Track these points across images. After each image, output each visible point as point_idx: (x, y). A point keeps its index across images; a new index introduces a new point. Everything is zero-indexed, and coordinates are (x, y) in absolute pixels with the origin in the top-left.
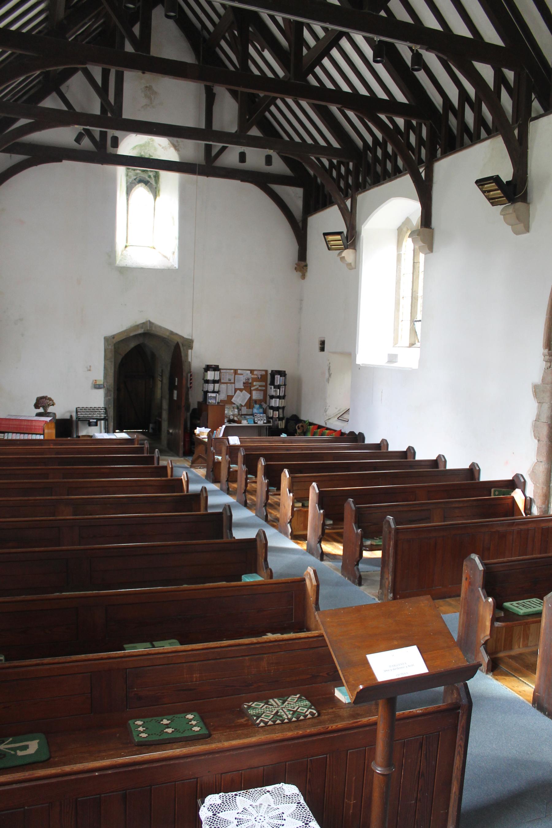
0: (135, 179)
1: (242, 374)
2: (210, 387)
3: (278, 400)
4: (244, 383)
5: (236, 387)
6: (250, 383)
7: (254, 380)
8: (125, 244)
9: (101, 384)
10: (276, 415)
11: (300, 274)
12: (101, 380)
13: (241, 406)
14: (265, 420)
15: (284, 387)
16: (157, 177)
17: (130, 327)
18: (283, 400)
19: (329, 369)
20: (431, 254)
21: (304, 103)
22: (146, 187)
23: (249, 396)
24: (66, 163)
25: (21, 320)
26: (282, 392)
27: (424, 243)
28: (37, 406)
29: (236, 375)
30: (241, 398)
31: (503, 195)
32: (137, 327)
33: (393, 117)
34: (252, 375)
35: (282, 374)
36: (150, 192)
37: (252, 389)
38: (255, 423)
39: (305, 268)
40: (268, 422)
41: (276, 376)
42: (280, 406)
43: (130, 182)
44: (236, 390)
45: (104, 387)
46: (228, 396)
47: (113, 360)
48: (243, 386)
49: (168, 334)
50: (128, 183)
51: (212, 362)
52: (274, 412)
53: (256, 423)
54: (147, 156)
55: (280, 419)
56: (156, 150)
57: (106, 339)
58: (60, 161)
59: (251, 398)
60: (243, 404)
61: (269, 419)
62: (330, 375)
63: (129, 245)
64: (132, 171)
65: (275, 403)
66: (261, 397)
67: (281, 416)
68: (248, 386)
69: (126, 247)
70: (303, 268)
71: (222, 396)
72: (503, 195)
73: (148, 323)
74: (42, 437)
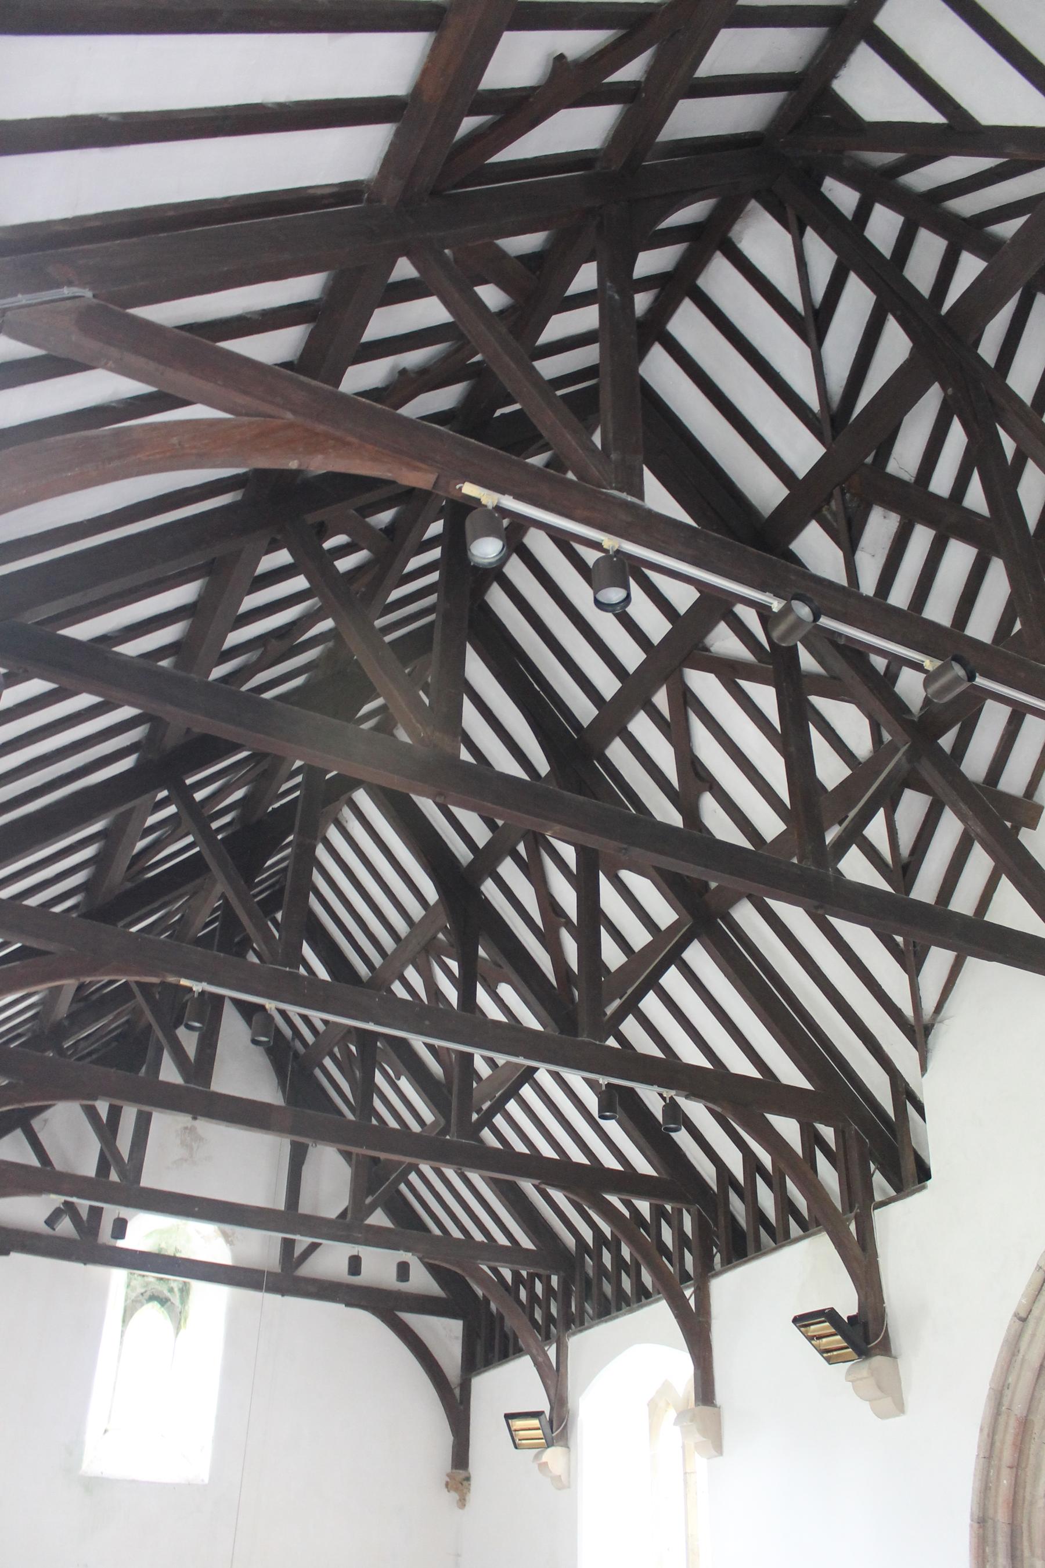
0: (142, 1294)
11: (455, 1496)
16: (185, 1291)
20: (721, 1458)
21: (475, 1177)
31: (846, 1344)
33: (633, 1201)
39: (465, 1483)
43: (133, 1298)
50: (129, 1301)
54: (170, 1252)
70: (462, 1484)
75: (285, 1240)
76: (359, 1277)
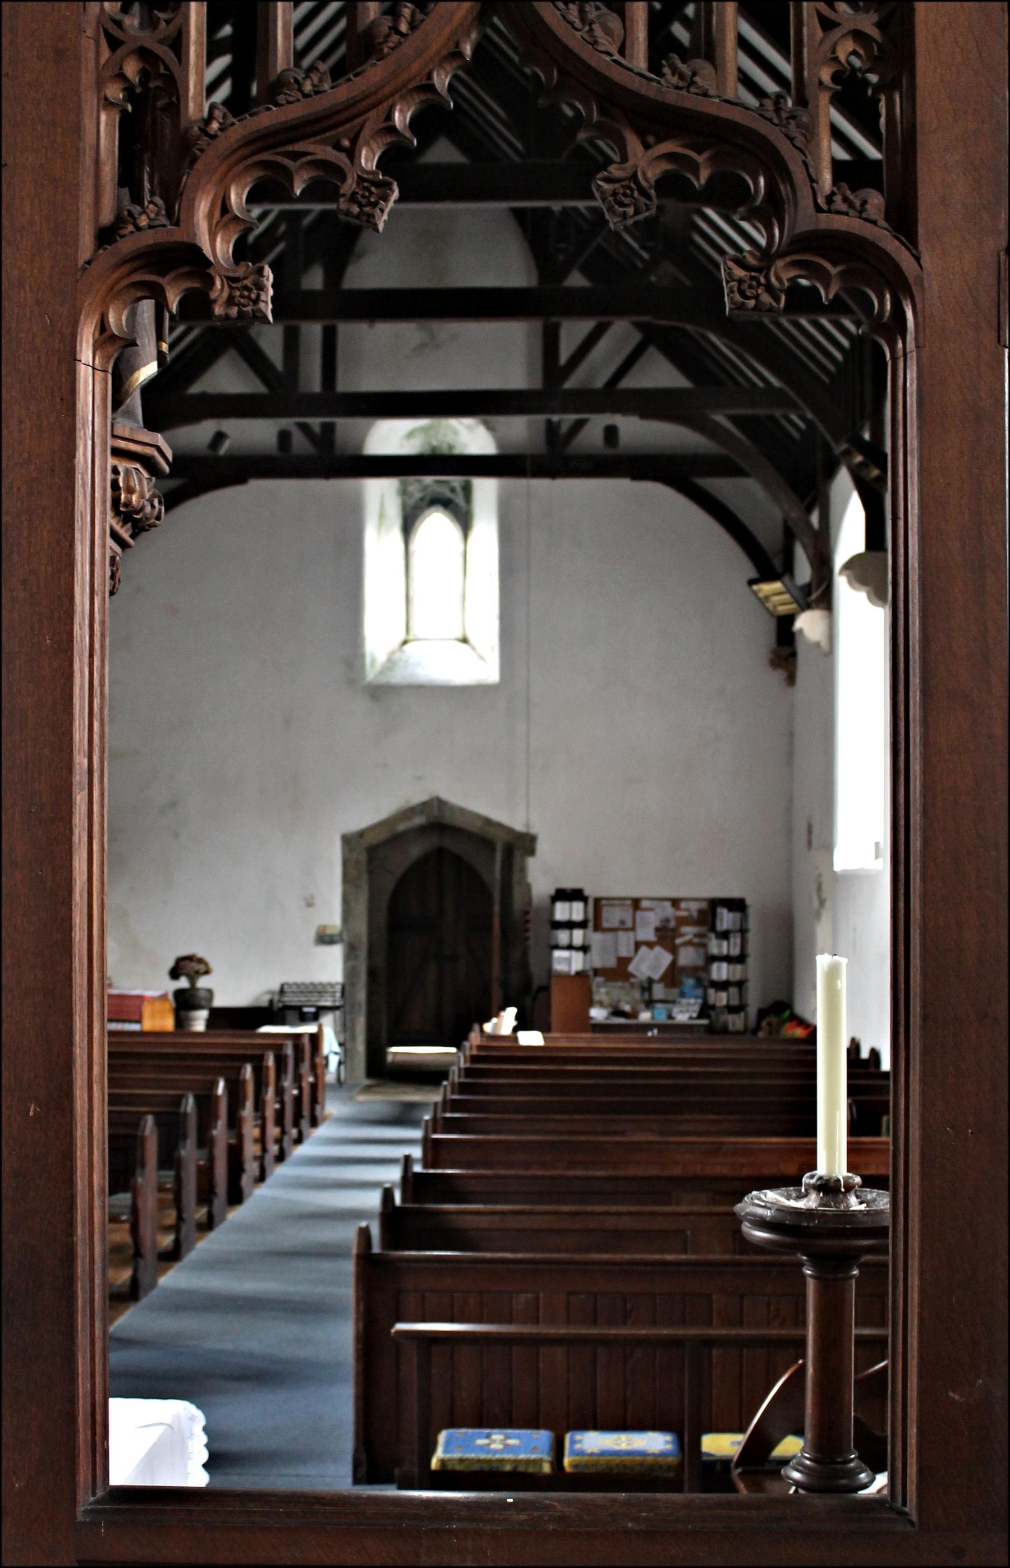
1: (650, 909)
2: (563, 936)
6: (673, 930)
7: (682, 921)
8: (402, 637)
10: (721, 1000)
11: (780, 675)
12: (334, 927)
13: (651, 981)
16: (467, 490)
19: (819, 889)
24: (256, 486)
25: (173, 804)
26: (735, 945)
28: (175, 973)
29: (639, 914)
35: (737, 905)
37: (679, 941)
40: (701, 1015)
44: (638, 945)
45: (341, 941)
49: (479, 823)
51: (569, 884)
55: (731, 1009)
56: (456, 433)
57: (348, 841)
59: (673, 964)
60: (656, 976)
61: (706, 1010)
62: (822, 903)
65: (719, 970)
66: (700, 962)
67: (735, 1002)
69: (405, 642)
71: (597, 959)
73: (435, 803)
74: (135, 1027)
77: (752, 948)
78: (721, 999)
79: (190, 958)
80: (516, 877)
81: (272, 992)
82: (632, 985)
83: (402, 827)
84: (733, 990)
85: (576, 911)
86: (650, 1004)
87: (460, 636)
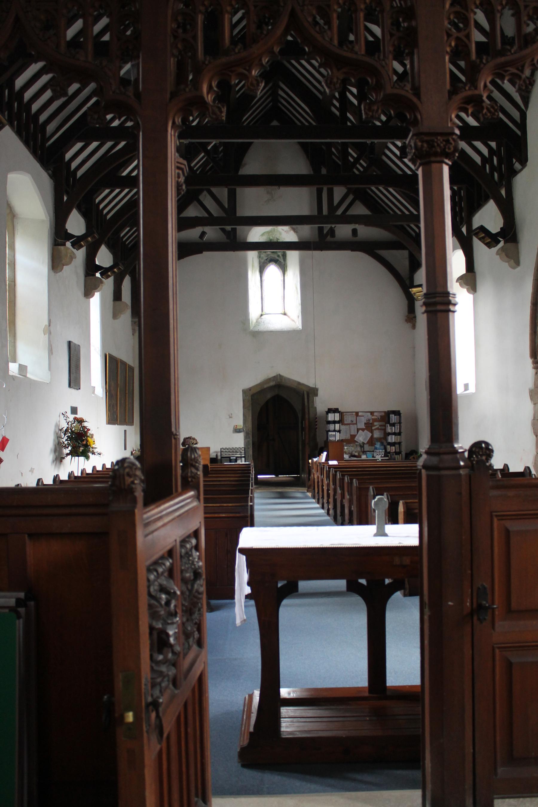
0: (266, 260)
2: (331, 427)
3: (394, 436)
4: (365, 424)
5: (358, 428)
6: (371, 424)
7: (375, 420)
8: (260, 313)
9: (241, 429)
10: (392, 450)
11: (410, 325)
12: (241, 425)
13: (364, 443)
14: (383, 454)
15: (399, 424)
16: (284, 256)
17: (263, 380)
18: (399, 436)
22: (276, 264)
23: (371, 434)
27: (468, 286)
29: (358, 417)
30: (362, 437)
31: (490, 240)
32: (269, 380)
34: (372, 416)
35: (397, 413)
36: (280, 269)
38: (373, 457)
39: (414, 319)
41: (391, 415)
42: (396, 441)
43: (263, 262)
44: (358, 430)
46: (351, 435)
47: (250, 408)
48: (365, 426)
50: (261, 263)
51: (333, 407)
52: (391, 447)
53: (375, 457)
56: (280, 234)
58: (201, 252)
59: (372, 436)
60: (366, 442)
61: (386, 454)
63: (265, 314)
64: (264, 253)
65: (391, 439)
66: (382, 436)
67: (398, 450)
68: (369, 426)
69: (261, 315)
70: (412, 319)
71: (344, 436)
72: (490, 240)
75: (319, 227)
76: (357, 238)
77: (402, 431)
78: (393, 449)
79: (190, 438)
80: (310, 406)
81: (217, 452)
82: (357, 445)
83: (265, 386)
84: (397, 446)
85: (337, 417)
86: (364, 452)
87: (283, 313)
